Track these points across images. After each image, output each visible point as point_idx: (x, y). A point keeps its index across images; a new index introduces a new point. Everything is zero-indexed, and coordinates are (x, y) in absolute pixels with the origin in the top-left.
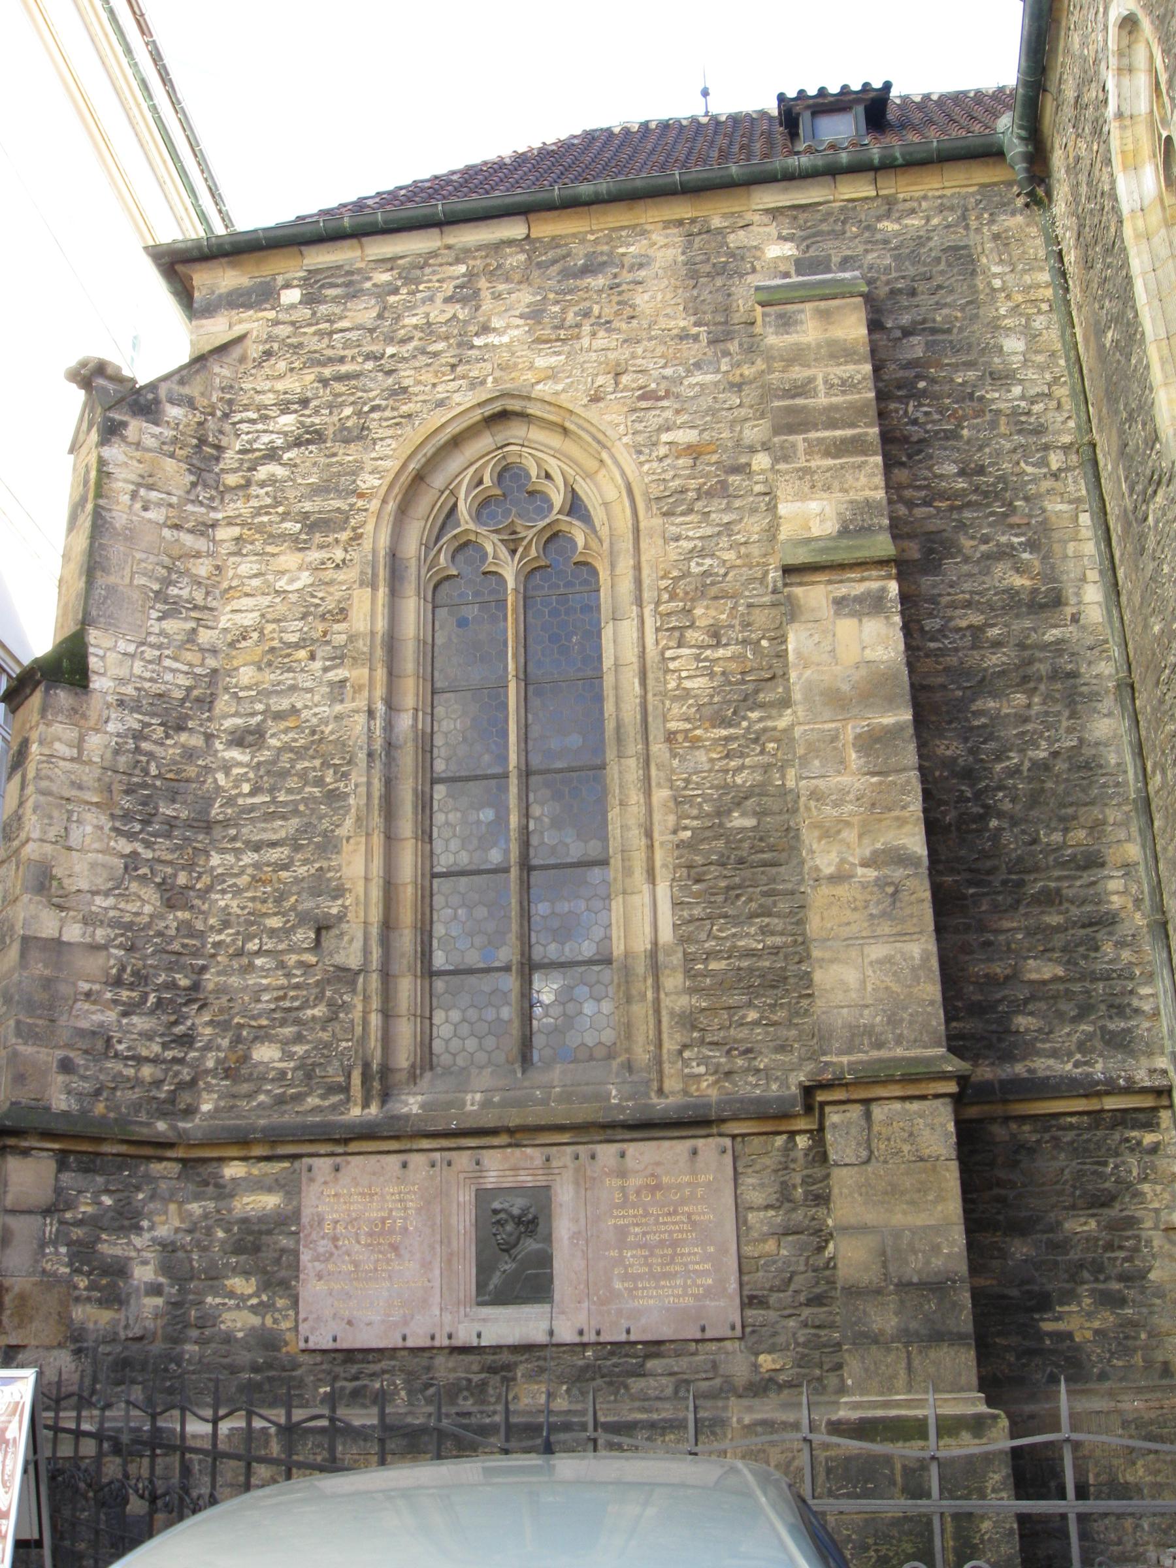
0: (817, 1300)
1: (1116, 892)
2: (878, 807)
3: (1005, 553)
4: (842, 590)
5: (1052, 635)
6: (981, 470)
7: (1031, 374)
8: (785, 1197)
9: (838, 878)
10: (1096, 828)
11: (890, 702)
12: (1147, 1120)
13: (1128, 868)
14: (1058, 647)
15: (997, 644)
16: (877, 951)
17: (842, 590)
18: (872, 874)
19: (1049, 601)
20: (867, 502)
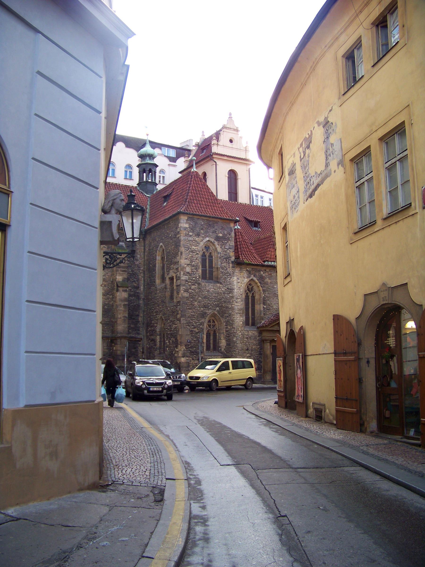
0: (110, 355)
1: (140, 319)
2: (124, 311)
3: (134, 281)
4: (123, 289)
5: (138, 291)
6: (133, 271)
7: (140, 260)
8: (108, 346)
9: (120, 318)
10: (139, 312)
11: (126, 301)
12: (140, 341)
13: (141, 317)
14: (138, 293)
15: (132, 291)
16: (123, 325)
17: (123, 289)
18: (123, 318)
19: (138, 288)
20: (125, 278)
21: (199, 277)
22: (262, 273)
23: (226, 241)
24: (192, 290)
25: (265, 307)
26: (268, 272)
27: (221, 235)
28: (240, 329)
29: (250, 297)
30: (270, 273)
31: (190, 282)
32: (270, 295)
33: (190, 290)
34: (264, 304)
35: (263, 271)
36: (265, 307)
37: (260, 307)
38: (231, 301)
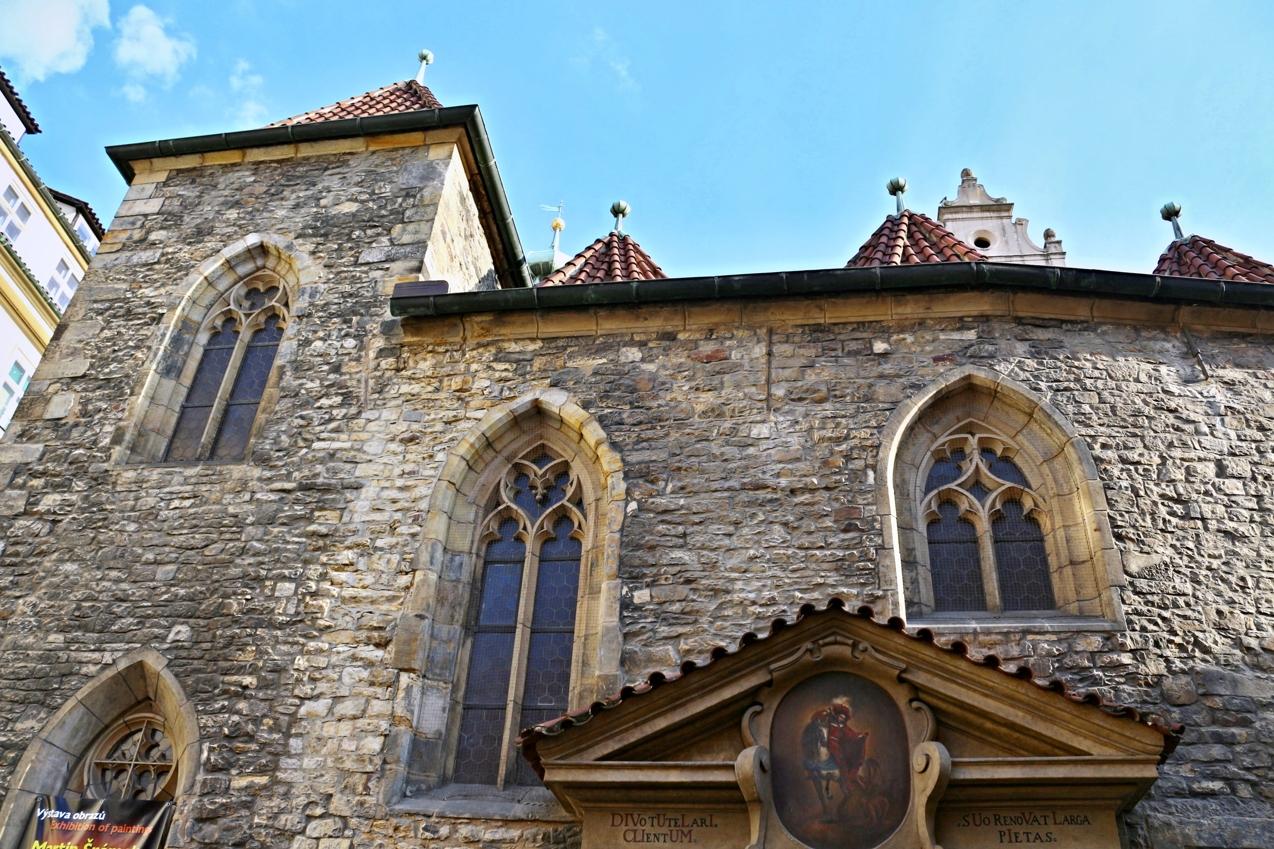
21: (117, 439)
22: (634, 354)
23: (369, 232)
24: (41, 516)
25: (641, 596)
26: (684, 344)
27: (350, 208)
28: (339, 804)
29: (531, 544)
30: (707, 348)
31: (44, 474)
32: (705, 500)
33: (21, 522)
34: (630, 573)
35: (642, 344)
36: (641, 596)
37: (597, 613)
38: (314, 571)
